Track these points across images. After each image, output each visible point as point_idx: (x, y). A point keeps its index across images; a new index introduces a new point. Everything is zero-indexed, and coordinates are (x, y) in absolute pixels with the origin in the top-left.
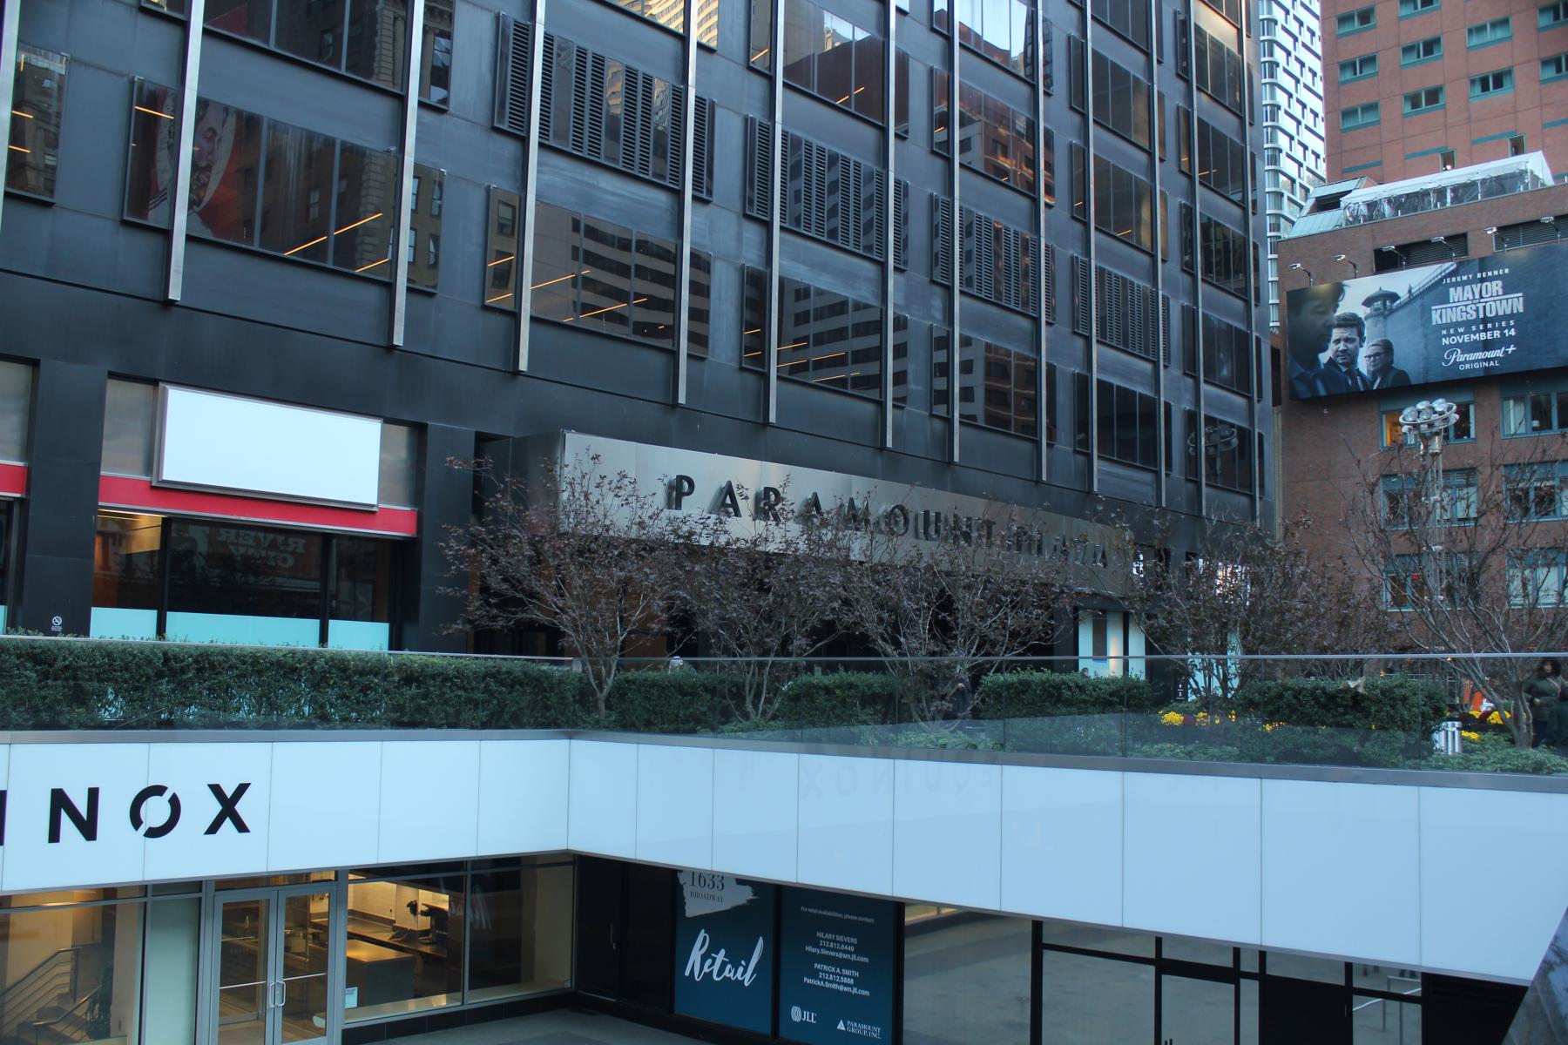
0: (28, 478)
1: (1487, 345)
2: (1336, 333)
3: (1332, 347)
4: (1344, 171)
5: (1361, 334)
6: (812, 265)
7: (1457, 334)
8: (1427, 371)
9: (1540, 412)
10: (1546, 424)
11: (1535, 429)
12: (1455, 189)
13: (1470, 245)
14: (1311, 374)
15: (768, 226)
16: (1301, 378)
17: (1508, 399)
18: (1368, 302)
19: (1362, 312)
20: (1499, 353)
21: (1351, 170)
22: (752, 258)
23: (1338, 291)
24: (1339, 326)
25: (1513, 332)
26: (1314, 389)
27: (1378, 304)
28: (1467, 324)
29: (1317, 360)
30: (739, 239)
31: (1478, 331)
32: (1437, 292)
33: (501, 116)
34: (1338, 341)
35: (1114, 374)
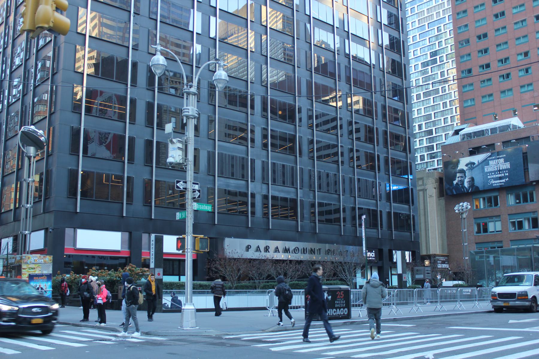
0: (131, 253)
1: (500, 178)
2: (458, 175)
3: (457, 179)
4: (465, 120)
5: (465, 175)
6: (279, 191)
7: (492, 175)
8: (484, 186)
9: (517, 197)
10: (520, 202)
11: (518, 203)
12: (491, 129)
13: (496, 147)
14: (451, 187)
15: (268, 184)
16: (449, 189)
17: (508, 194)
18: (467, 165)
19: (465, 168)
20: (504, 181)
21: (467, 120)
22: (264, 192)
23: (458, 162)
24: (459, 173)
25: (507, 174)
26: (452, 192)
27: (469, 166)
28: (495, 172)
29: (453, 183)
30: (262, 188)
32: (485, 162)
33: (210, 172)
34: (459, 177)
35: (364, 205)
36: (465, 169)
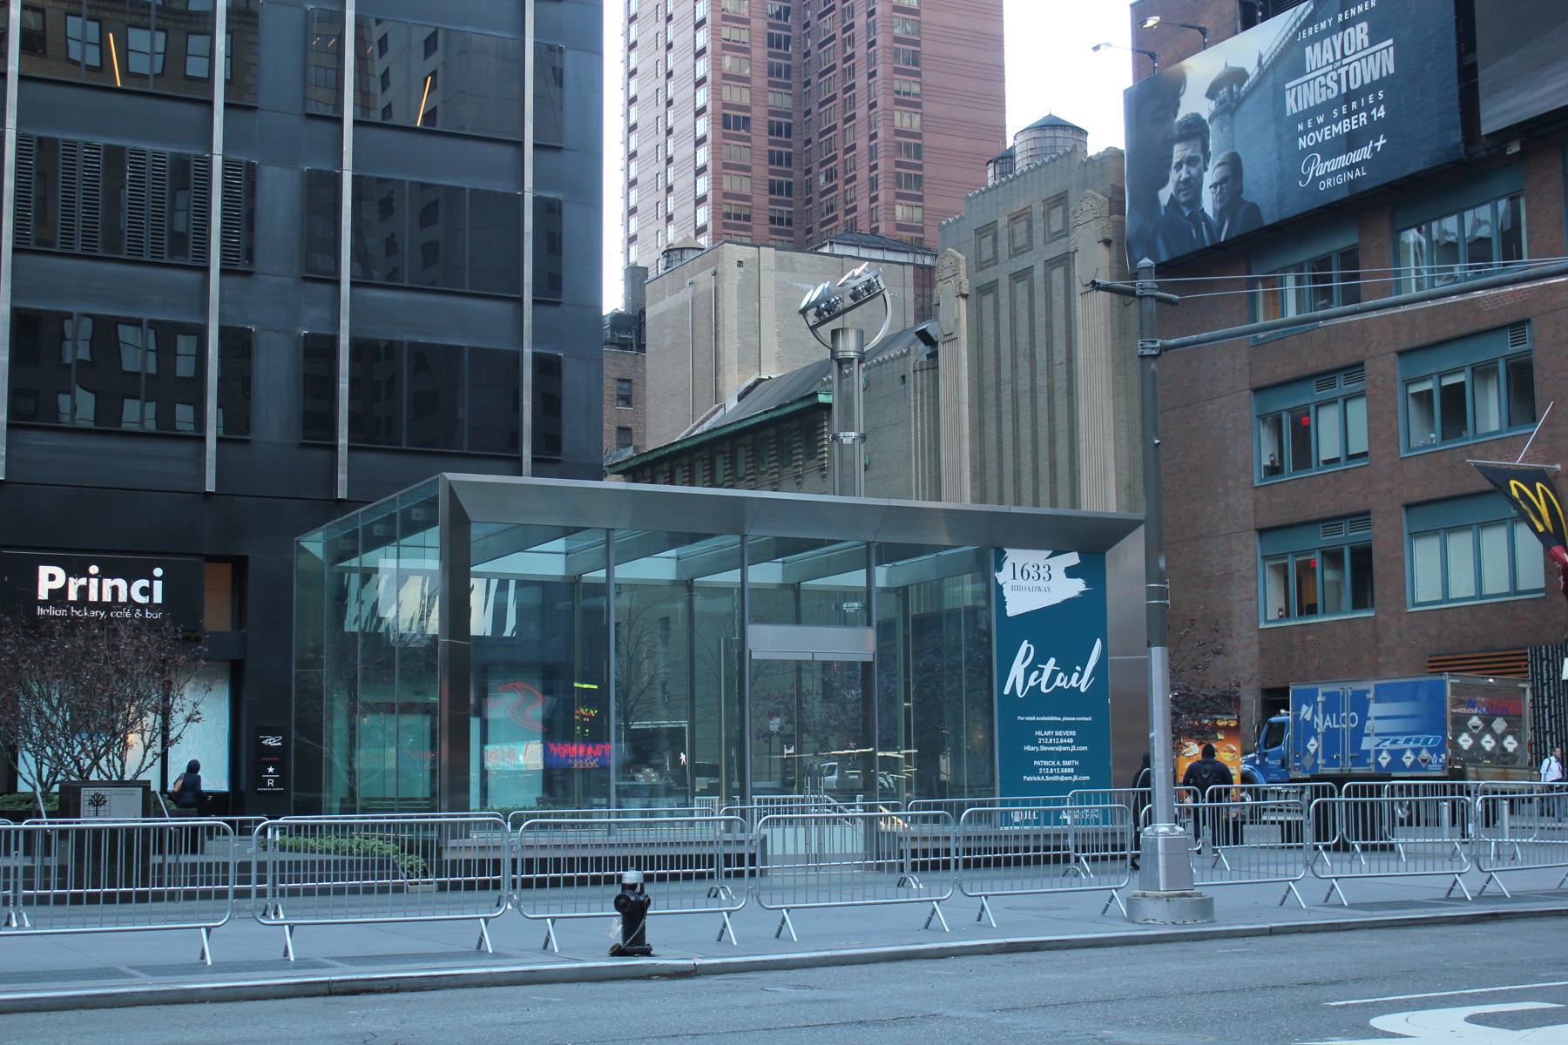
1: (1351, 141)
2: (1179, 152)
3: (1174, 176)
5: (1205, 148)
18: (1211, 94)
19: (1205, 109)
20: (1364, 153)
24: (1183, 138)
27: (1223, 92)
28: (1326, 108)
31: (1341, 118)
34: (1179, 166)
36: (1206, 116)
